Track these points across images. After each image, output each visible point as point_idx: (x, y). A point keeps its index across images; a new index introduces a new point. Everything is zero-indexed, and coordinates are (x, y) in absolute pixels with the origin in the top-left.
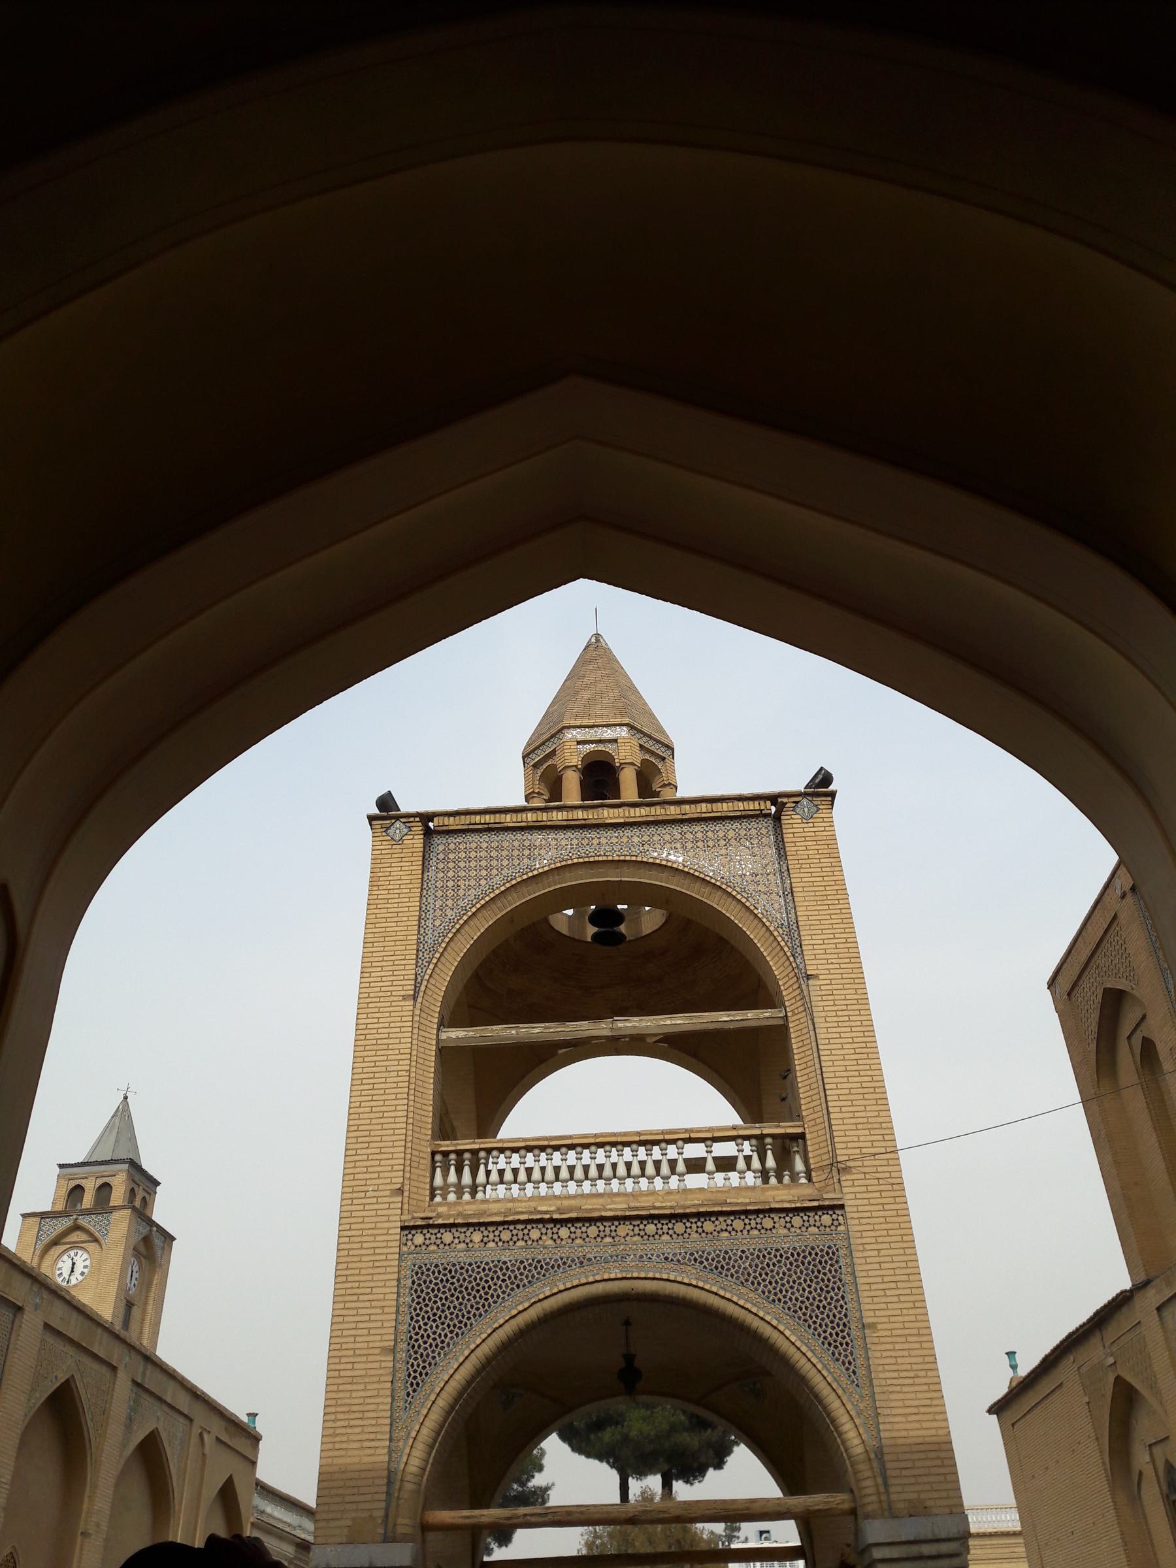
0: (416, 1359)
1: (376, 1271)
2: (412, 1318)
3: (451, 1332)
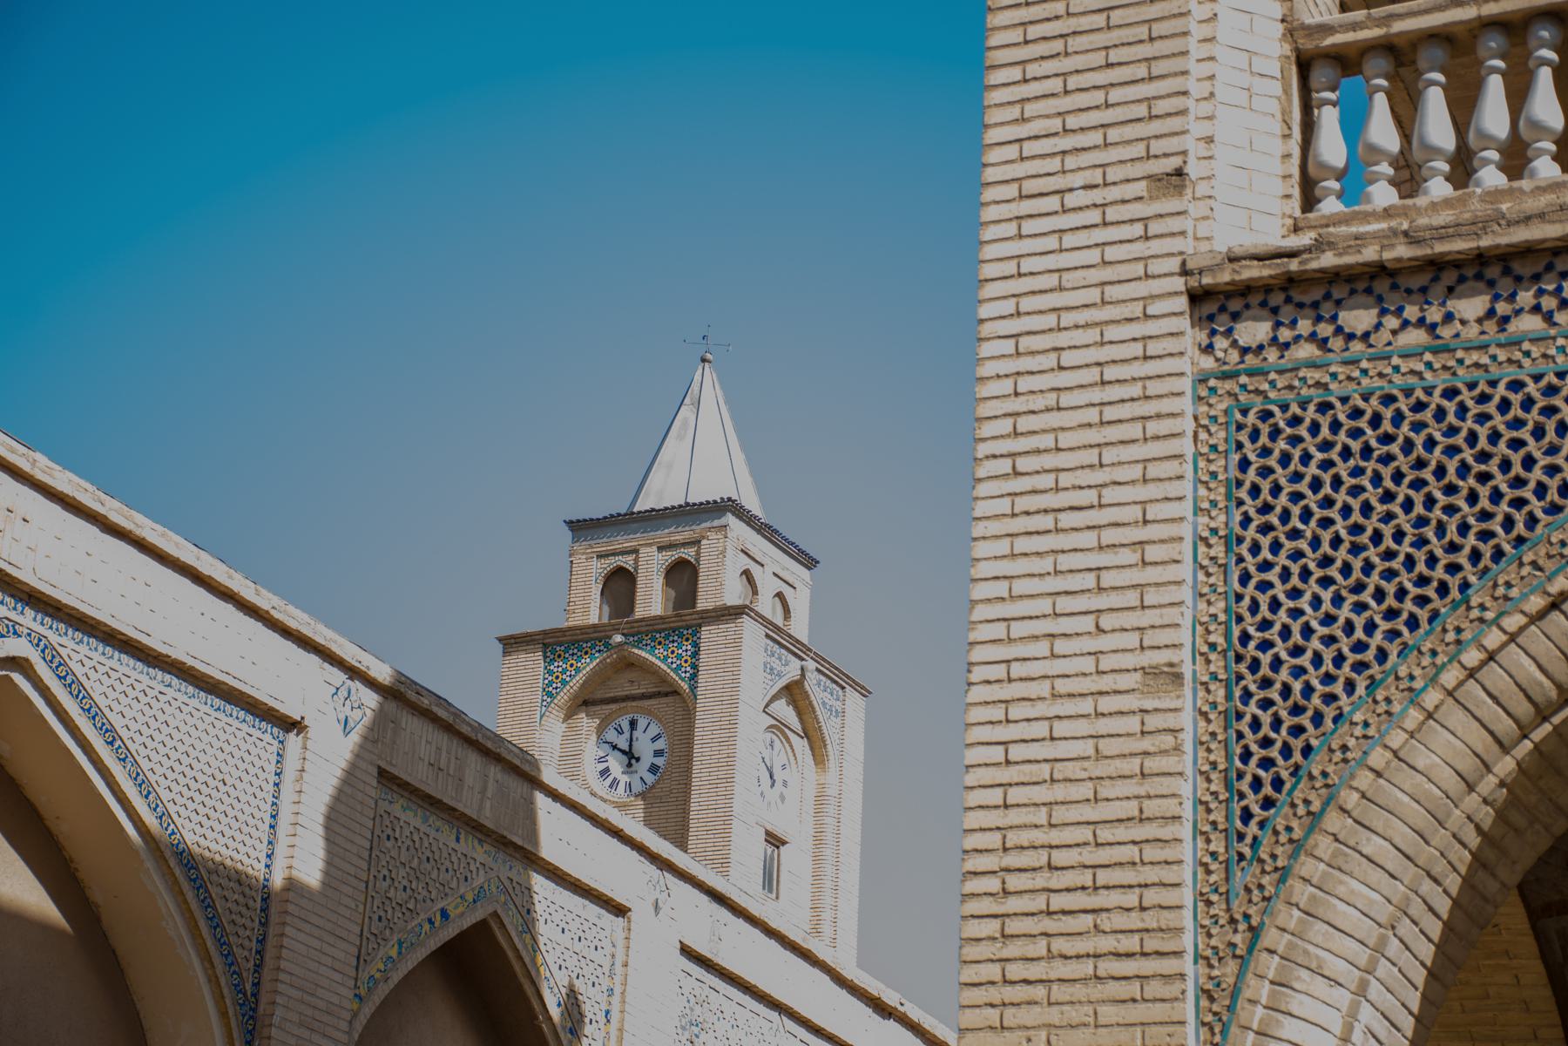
1: (1113, 433)
3: (1391, 614)
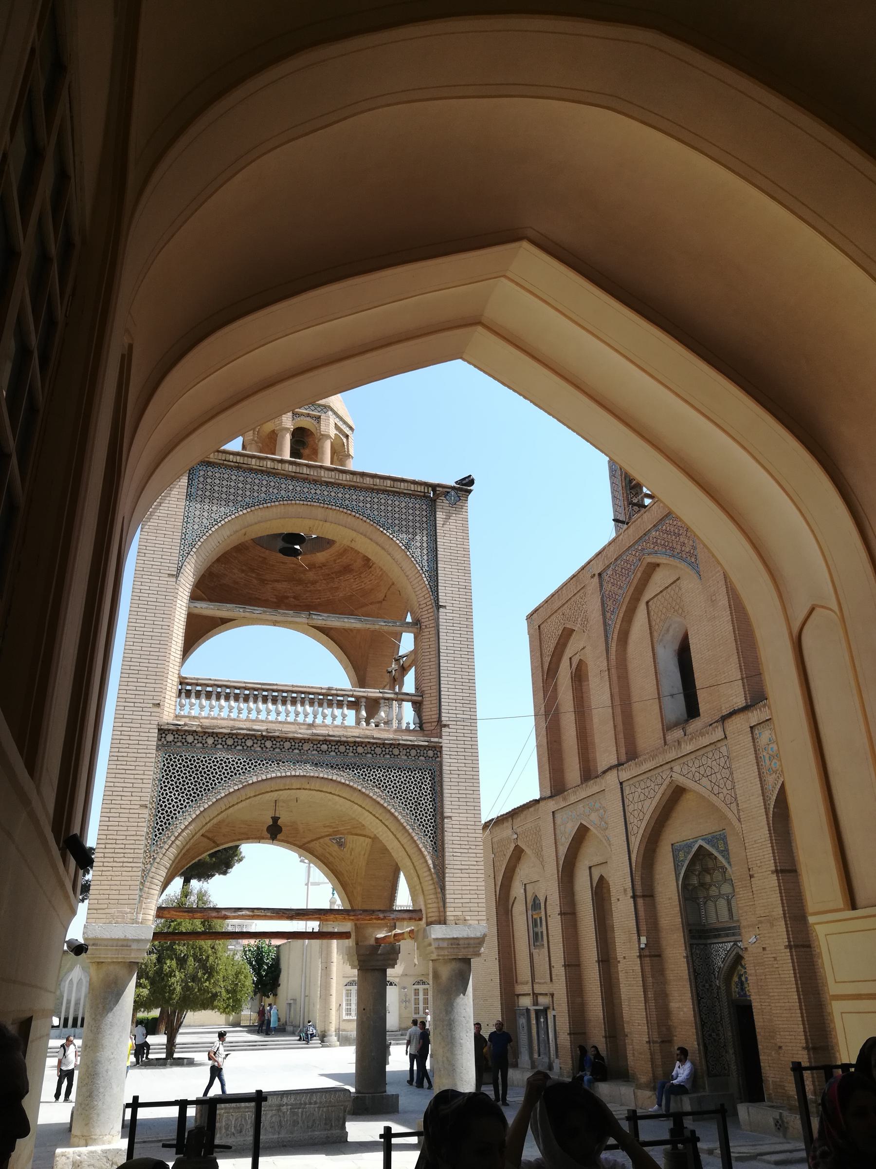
0: (162, 814)
2: (161, 788)
